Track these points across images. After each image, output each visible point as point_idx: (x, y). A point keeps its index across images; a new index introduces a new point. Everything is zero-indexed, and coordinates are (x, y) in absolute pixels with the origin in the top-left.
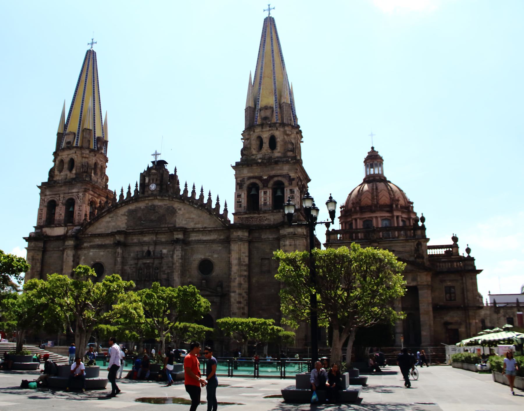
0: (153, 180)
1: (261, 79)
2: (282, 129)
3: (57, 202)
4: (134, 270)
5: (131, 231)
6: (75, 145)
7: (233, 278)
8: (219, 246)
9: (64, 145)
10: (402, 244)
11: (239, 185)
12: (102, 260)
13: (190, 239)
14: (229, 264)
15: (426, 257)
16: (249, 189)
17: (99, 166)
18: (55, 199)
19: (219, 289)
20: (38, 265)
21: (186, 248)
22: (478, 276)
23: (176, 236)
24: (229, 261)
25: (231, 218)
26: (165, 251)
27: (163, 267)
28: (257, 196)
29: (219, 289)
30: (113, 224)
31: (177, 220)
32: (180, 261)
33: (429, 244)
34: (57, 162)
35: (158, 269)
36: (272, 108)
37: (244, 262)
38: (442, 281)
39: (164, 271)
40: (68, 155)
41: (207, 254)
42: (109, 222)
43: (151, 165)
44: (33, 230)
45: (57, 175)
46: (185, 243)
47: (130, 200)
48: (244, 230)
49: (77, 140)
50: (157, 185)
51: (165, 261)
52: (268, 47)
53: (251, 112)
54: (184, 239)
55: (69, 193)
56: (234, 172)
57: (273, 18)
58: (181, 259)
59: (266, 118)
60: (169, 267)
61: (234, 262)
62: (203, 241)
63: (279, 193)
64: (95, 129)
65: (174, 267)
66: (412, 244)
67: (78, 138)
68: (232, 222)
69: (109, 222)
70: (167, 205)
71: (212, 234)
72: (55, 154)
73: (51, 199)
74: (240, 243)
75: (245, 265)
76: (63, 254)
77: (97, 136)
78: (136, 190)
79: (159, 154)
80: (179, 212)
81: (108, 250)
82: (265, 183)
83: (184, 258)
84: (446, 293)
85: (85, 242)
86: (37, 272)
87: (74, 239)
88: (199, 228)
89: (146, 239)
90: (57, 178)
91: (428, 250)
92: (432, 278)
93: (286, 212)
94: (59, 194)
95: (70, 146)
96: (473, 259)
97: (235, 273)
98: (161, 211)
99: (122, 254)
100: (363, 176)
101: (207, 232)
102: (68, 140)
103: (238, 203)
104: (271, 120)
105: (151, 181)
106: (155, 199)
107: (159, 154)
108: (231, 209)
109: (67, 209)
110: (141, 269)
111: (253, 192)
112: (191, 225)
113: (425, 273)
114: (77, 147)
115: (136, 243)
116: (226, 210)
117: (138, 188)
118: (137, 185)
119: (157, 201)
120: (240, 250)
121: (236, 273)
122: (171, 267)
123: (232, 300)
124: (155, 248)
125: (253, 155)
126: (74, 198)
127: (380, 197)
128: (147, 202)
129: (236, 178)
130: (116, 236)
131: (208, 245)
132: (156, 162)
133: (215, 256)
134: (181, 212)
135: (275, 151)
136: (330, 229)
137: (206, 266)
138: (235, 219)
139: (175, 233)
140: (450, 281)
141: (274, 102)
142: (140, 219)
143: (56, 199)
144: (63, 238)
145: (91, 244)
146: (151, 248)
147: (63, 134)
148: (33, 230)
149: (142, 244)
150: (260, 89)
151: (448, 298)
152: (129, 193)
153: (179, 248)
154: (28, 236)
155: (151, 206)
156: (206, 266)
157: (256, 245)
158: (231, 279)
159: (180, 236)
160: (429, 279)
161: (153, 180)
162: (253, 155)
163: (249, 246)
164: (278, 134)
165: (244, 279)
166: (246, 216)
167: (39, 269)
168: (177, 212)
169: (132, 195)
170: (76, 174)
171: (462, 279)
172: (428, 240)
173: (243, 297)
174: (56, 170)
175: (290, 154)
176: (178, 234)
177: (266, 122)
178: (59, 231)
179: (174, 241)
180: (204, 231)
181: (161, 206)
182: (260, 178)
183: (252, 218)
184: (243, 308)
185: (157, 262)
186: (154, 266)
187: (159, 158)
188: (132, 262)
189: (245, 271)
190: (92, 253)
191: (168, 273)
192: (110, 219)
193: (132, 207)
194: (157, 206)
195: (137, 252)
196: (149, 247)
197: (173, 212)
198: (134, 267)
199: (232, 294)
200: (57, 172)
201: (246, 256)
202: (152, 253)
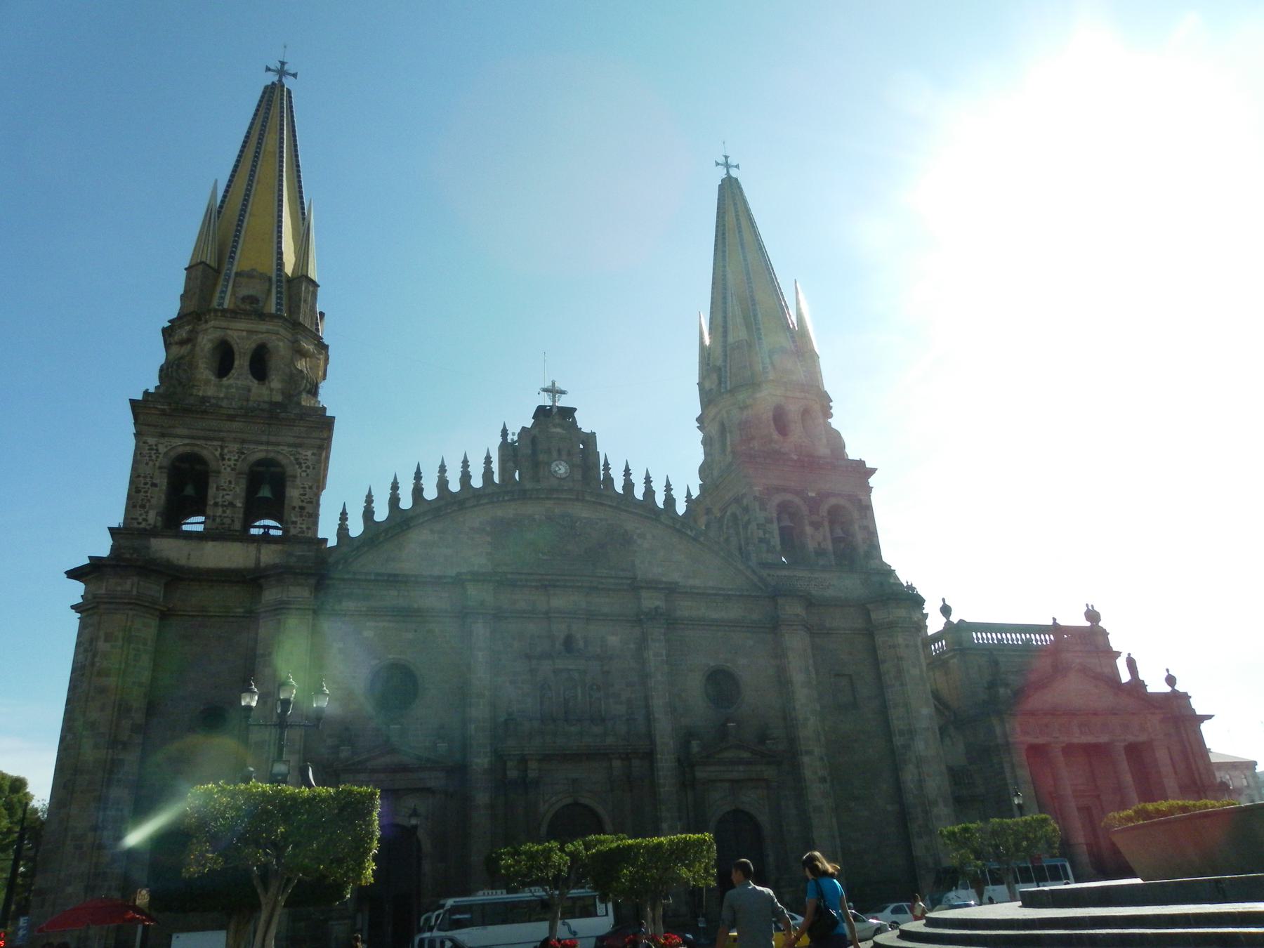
3: (213, 465)
18: (205, 453)
20: (145, 661)
26: (613, 640)
34: (206, 342)
40: (250, 332)
50: (572, 466)
61: (798, 678)
63: (839, 532)
73: (188, 449)
79: (563, 392)
89: (560, 601)
94: (222, 440)
102: (244, 292)
105: (555, 454)
106: (577, 499)
107: (563, 392)
111: (787, 523)
123: (808, 773)
126: (284, 462)
136: (954, 618)
139: (644, 594)
143: (209, 452)
161: (559, 451)
169: (496, 479)
187: (563, 402)
193: (508, 511)
202: (581, 644)
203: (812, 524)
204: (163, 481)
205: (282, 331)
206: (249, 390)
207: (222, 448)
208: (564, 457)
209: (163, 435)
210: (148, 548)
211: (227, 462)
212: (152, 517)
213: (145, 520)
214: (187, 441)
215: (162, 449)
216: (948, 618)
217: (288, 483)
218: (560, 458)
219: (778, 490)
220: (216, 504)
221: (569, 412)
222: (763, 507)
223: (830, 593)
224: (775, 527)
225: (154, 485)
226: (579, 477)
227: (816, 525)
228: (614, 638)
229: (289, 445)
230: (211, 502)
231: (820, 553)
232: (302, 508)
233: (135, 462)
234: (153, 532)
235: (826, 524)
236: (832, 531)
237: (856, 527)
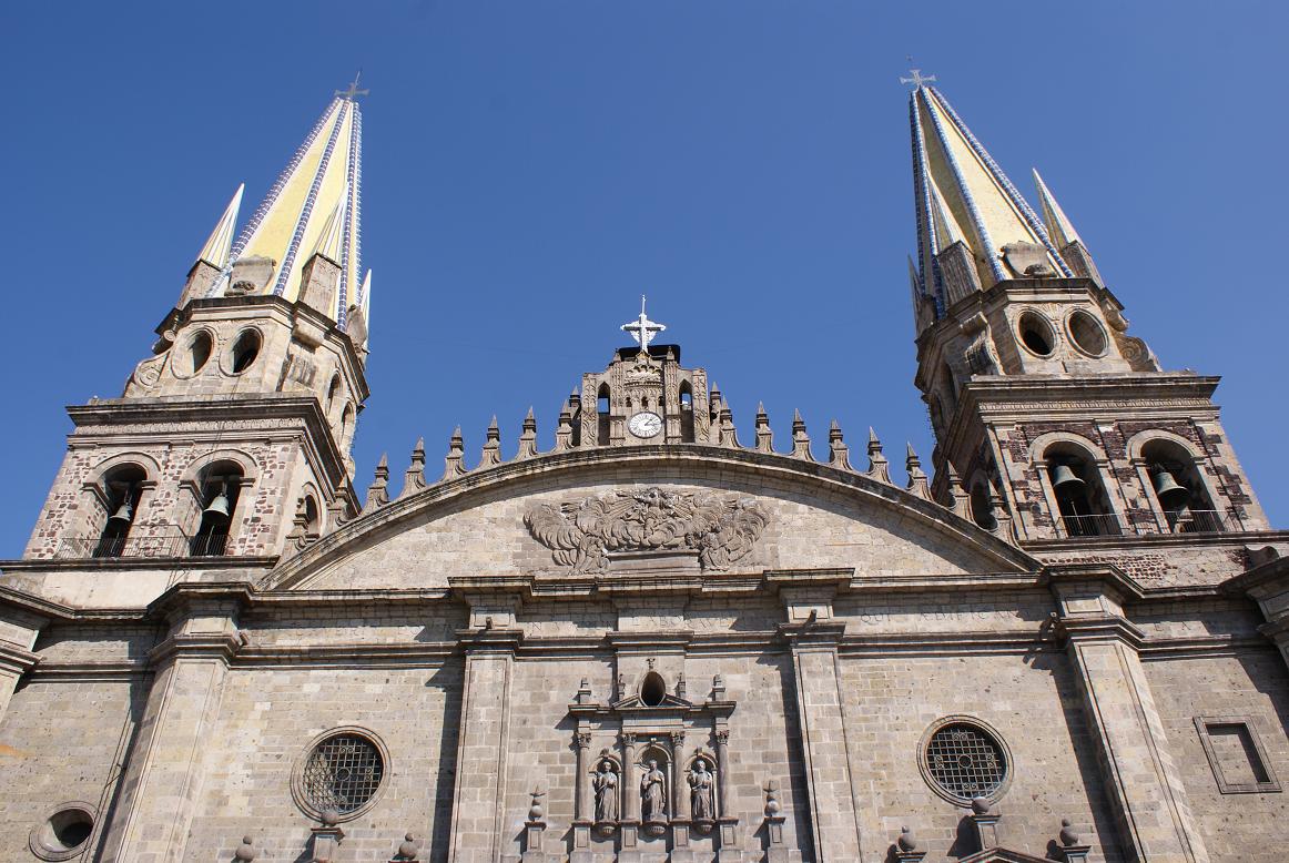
0: (645, 402)
6: (269, 291)
8: (1009, 664)
12: (371, 724)
18: (145, 463)
23: (797, 614)
27: (736, 759)
31: (783, 551)
62: (931, 637)
63: (1170, 483)
65: (809, 750)
69: (429, 547)
73: (125, 459)
74: (1118, 642)
97: (1138, 779)
105: (637, 405)
111: (1066, 475)
125: (1031, 364)
133: (1002, 706)
137: (963, 754)
146: (667, 666)
161: (645, 402)
162: (1031, 364)
168: (777, 519)
178: (137, 590)
186: (686, 752)
190: (315, 681)
192: (434, 536)
198: (563, 759)
202: (671, 690)
203: (1115, 473)
205: (274, 313)
207: (167, 453)
211: (169, 471)
213: (50, 551)
215: (94, 462)
217: (243, 489)
222: (1017, 455)
223: (1168, 581)
226: (677, 432)
227: (1122, 475)
228: (738, 677)
232: (256, 520)
235: (1142, 471)
236: (1157, 484)
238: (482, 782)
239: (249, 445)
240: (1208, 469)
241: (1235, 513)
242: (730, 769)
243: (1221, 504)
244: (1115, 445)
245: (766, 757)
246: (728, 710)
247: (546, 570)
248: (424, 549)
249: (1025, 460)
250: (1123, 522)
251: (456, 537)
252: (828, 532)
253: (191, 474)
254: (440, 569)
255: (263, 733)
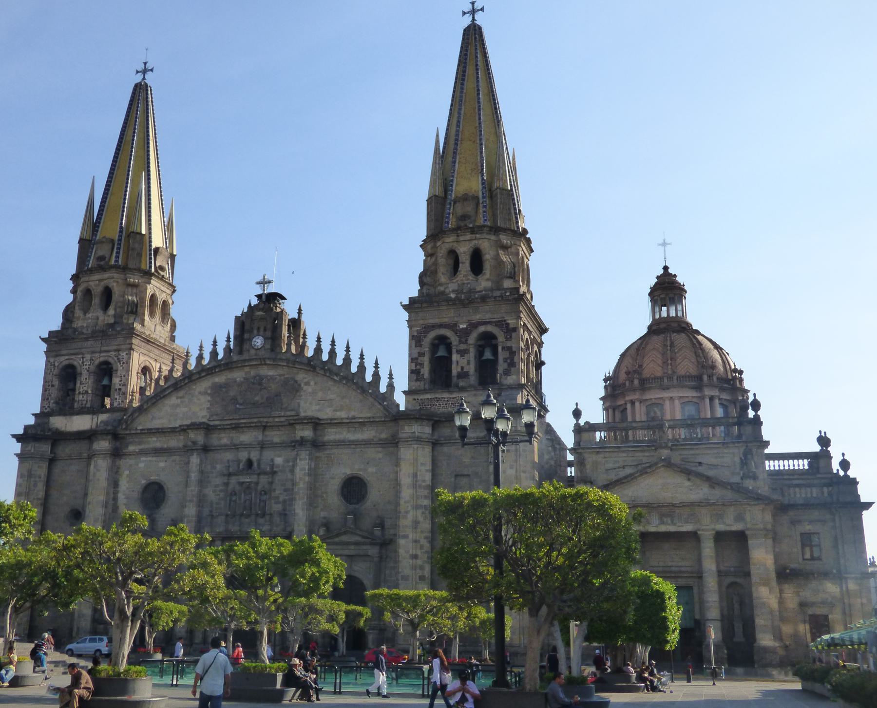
0: (259, 329)
1: (456, 144)
2: (493, 238)
3: (79, 369)
4: (222, 495)
5: (217, 423)
6: (113, 262)
7: (403, 511)
8: (378, 452)
9: (91, 263)
10: (715, 451)
11: (416, 340)
12: (163, 478)
13: (326, 438)
14: (396, 485)
15: (762, 476)
16: (434, 347)
17: (160, 302)
18: (75, 363)
19: (377, 532)
20: (41, 486)
21: (318, 454)
22: (866, 514)
24: (397, 480)
25: (400, 400)
26: (279, 461)
27: (274, 490)
28: (448, 359)
29: (377, 532)
30: (185, 410)
31: (302, 404)
32: (307, 479)
33: (767, 451)
34: (79, 293)
35: (266, 494)
36: (477, 198)
37: (424, 481)
38: (794, 523)
39: (278, 498)
40: (100, 280)
41: (356, 467)
42: (178, 406)
43: (255, 301)
44: (31, 421)
45: (78, 318)
46: (316, 445)
47: (216, 366)
48: (424, 423)
49: (118, 253)
50: (265, 338)
51: (278, 478)
52: (470, 84)
53: (438, 205)
54: (315, 438)
55: (100, 352)
56: (405, 315)
57: (480, 28)
58: (309, 475)
59: (464, 217)
60: (285, 490)
61: (405, 480)
62: (350, 441)
63: (488, 355)
64: (150, 233)
65: (296, 490)
66: (736, 451)
67: (119, 249)
68: (402, 408)
69: (178, 406)
70: (283, 375)
71: (365, 429)
72: (75, 278)
73: (67, 362)
74: (415, 446)
75: (427, 487)
76: (89, 465)
77: (154, 246)
78: (228, 346)
79: (269, 282)
80: (305, 388)
81: (174, 458)
82: (464, 334)
83: (314, 474)
84: (803, 546)
85: (131, 443)
86: (38, 499)
87: (109, 437)
88: (342, 419)
89: (246, 437)
90: (78, 324)
91: (767, 462)
92: (774, 516)
93: (458, 423)
95: (103, 266)
96: (854, 482)
97: (405, 502)
98: (273, 387)
99: (201, 464)
100: (648, 321)
101: (357, 425)
102: (100, 253)
103: (414, 373)
104: (475, 221)
105: (255, 332)
106: (261, 364)
107: (269, 282)
108: (402, 383)
109: (98, 380)
110: (235, 494)
111: (442, 352)
112: (326, 413)
113: (761, 507)
114: (116, 267)
115: (225, 445)
116: (391, 387)
117: (232, 344)
118: (229, 338)
119: (265, 367)
120: (416, 460)
121: (408, 502)
122: (290, 490)
123: (401, 551)
124: (261, 455)
125: (441, 285)
126: (111, 360)
127: (678, 361)
128: (247, 369)
129: (410, 327)
130: (190, 431)
131: (358, 450)
132: (264, 297)
133: (371, 470)
134: (309, 389)
135: (480, 277)
136: (582, 422)
137: (353, 489)
138: (407, 402)
139: (298, 427)
140: (811, 522)
141: (481, 187)
142: (234, 400)
143: (77, 361)
144: (88, 436)
145: (143, 447)
146: (254, 455)
147: (90, 241)
148: (31, 421)
149: (236, 447)
150: (454, 162)
151: (808, 556)
152: (214, 353)
153: (304, 454)
154: (21, 431)
155: (254, 377)
156: (353, 489)
157: (446, 449)
158: (400, 512)
159: (307, 433)
160: (769, 517)
161: (259, 329)
163: (433, 450)
164: (486, 244)
165: (423, 513)
166: (429, 396)
167: (41, 494)
169: (221, 356)
170: (115, 316)
171: (834, 520)
172: (767, 444)
173: (422, 547)
174: (77, 308)
175: (507, 284)
176: (303, 430)
177: (465, 226)
178: (81, 423)
179: (297, 441)
180: (351, 423)
181: (272, 378)
182: (453, 327)
183: (438, 400)
184: (422, 568)
185: (264, 480)
186: (260, 487)
187: (271, 289)
188: (219, 481)
189: (426, 497)
190: (143, 463)
191: (285, 501)
192: (179, 401)
193: (220, 379)
194: (266, 376)
195: (228, 461)
196: (249, 453)
197: (294, 388)
198: (221, 491)
199: (402, 542)
200: (78, 313)
201: (427, 471)
202: (255, 464)
203: (458, 352)
204: (56, 382)
205: (115, 275)
206: (98, 318)
208: (262, 333)
209: (57, 356)
210: (48, 423)
212: (53, 405)
214: (67, 357)
216: (577, 421)
218: (258, 335)
219: (433, 327)
220: (79, 393)
221: (275, 297)
224: (426, 360)
225: (53, 386)
227: (462, 353)
229: (115, 351)
230: (77, 392)
231: (463, 375)
232: (120, 389)
233: (45, 373)
234: (51, 414)
235: (472, 351)
236: (480, 353)
237: (500, 349)
238: (191, 501)
239: (113, 353)
240: (503, 348)
241: (507, 373)
242: (273, 494)
243: (501, 366)
244: (464, 334)
245: (285, 490)
246: (274, 473)
247: (217, 415)
248: (176, 406)
249: (421, 346)
250: (455, 380)
251: (186, 400)
252: (320, 395)
253: (92, 368)
254: (181, 415)
255: (128, 482)
